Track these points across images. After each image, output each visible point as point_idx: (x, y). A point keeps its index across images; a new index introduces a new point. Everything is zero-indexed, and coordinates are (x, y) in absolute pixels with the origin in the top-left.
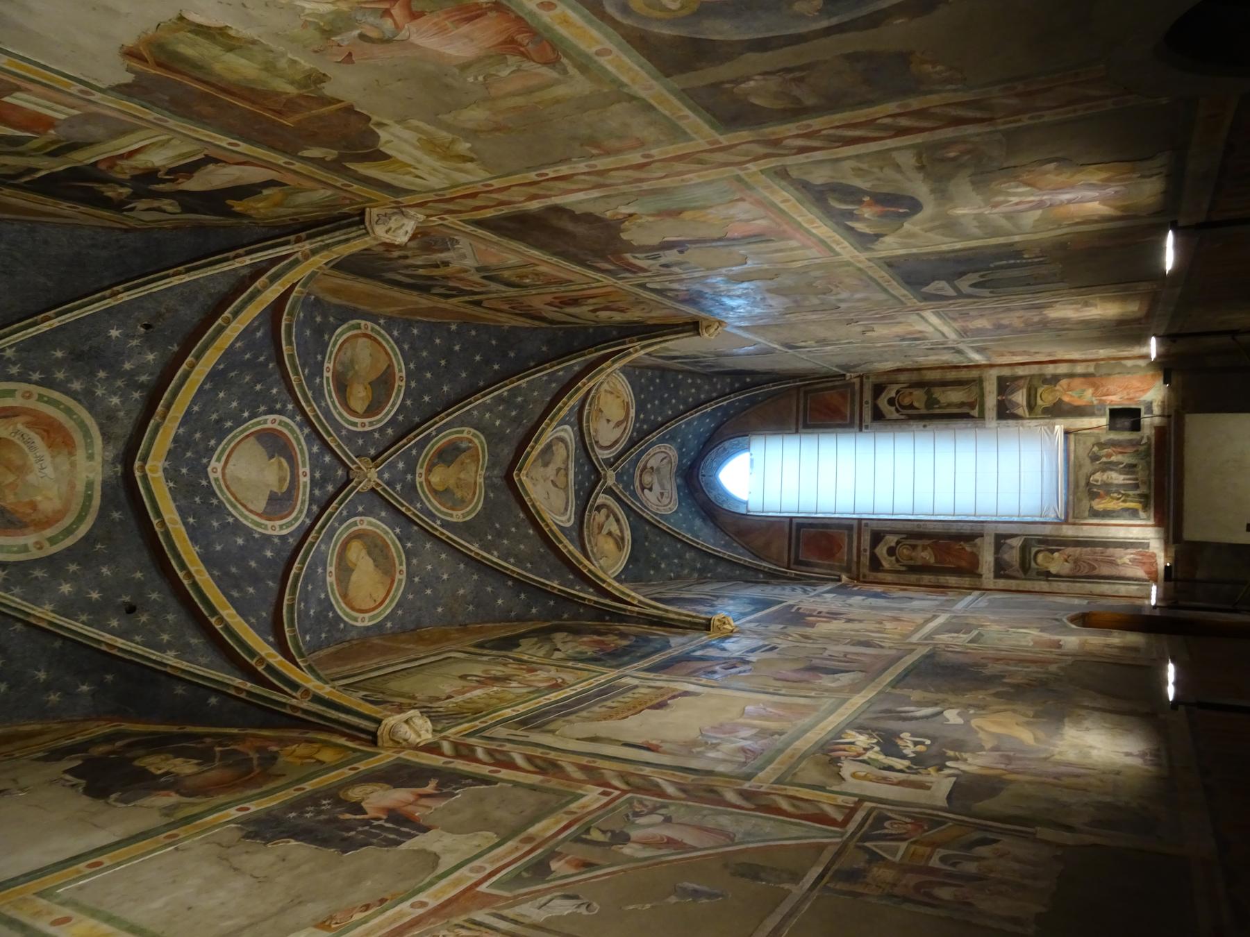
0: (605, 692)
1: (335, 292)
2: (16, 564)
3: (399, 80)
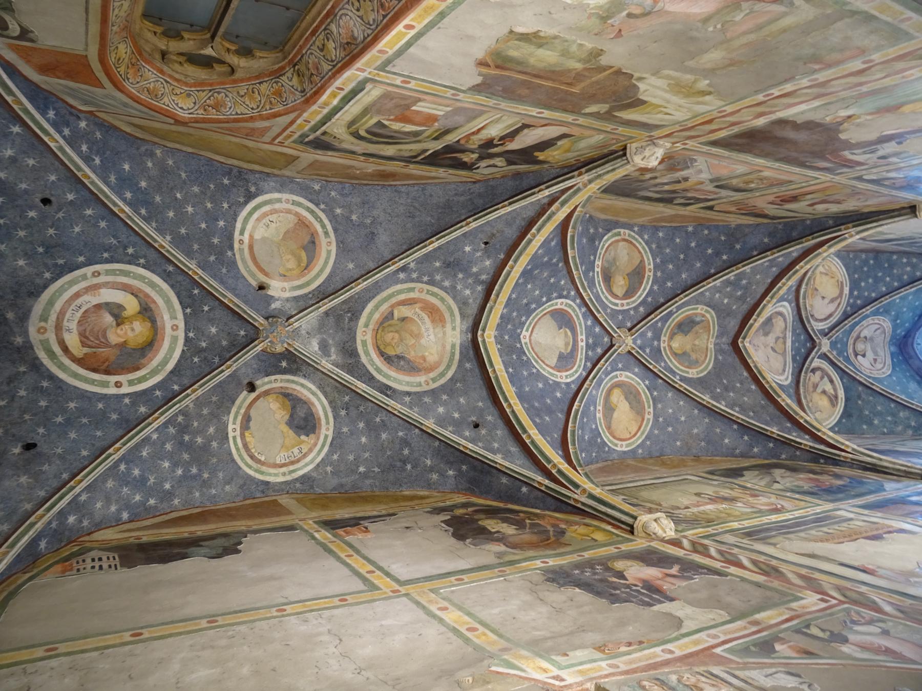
0: (820, 520)
1: (603, 210)
2: (416, 393)
3: (655, 42)
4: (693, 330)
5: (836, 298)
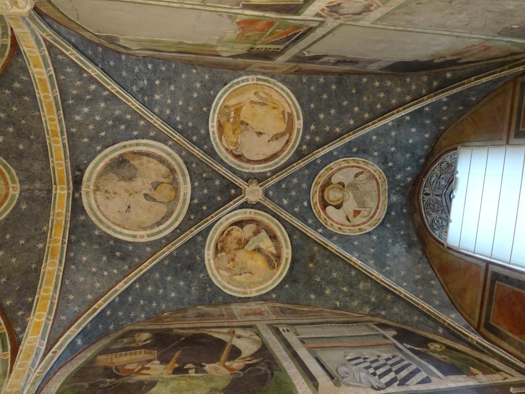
5: (283, 134)
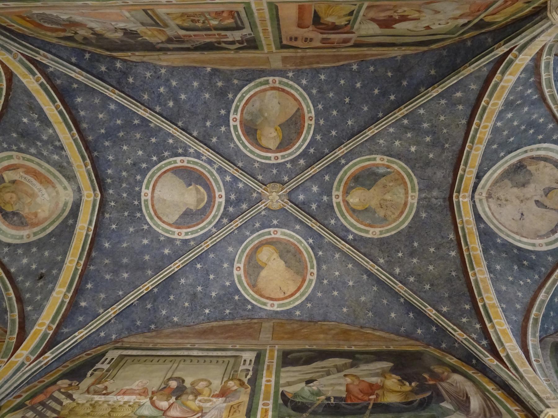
4: (379, 182)
